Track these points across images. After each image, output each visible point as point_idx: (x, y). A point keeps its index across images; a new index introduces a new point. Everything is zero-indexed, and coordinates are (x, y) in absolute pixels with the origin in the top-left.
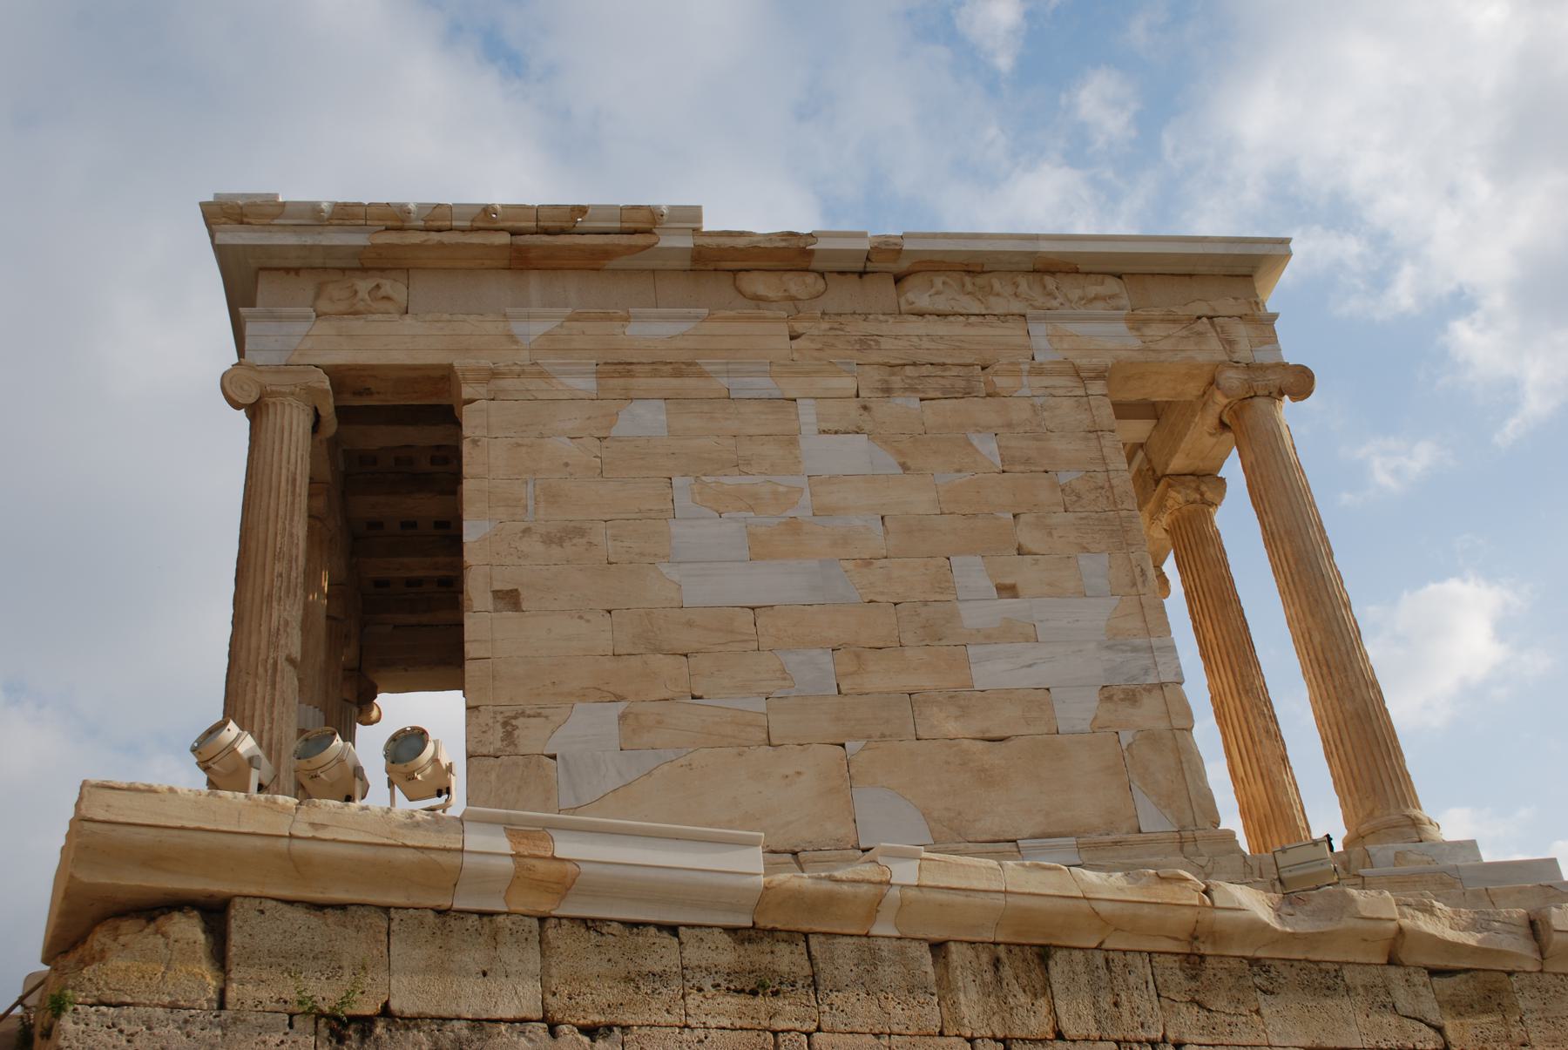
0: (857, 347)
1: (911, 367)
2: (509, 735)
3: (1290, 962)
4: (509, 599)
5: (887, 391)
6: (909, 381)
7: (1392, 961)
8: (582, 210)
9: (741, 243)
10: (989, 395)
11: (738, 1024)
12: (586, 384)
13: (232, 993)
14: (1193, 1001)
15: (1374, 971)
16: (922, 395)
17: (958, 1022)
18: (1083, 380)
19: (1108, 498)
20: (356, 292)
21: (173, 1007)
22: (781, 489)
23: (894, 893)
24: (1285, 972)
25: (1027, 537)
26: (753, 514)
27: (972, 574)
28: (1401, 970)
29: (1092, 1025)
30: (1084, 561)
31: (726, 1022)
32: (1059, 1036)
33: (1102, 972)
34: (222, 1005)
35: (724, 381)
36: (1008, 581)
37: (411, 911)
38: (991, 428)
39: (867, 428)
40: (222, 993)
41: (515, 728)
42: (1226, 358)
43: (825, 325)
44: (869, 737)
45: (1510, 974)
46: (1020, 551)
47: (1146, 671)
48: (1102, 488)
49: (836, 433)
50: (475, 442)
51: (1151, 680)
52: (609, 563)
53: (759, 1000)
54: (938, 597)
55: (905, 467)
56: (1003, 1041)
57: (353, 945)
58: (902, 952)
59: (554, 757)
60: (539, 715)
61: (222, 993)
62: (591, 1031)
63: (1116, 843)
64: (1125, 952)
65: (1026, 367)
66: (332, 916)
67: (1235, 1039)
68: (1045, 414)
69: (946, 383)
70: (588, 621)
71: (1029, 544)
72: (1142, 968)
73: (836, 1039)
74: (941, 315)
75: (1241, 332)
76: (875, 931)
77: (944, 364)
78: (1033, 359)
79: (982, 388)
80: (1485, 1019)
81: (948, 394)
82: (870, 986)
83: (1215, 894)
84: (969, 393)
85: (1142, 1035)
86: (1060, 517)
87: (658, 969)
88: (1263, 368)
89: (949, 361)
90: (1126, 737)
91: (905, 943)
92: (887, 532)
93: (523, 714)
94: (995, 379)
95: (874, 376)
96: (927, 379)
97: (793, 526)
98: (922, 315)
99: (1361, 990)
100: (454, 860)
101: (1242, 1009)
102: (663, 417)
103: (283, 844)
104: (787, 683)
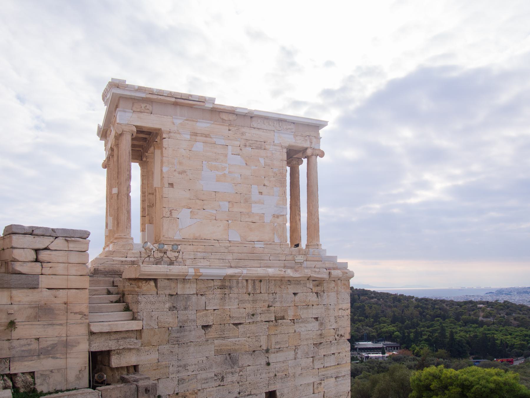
0: (241, 134)
1: (251, 141)
3: (294, 280)
5: (245, 146)
6: (250, 144)
7: (308, 279)
10: (264, 149)
11: (220, 293)
13: (158, 293)
14: (279, 287)
15: (305, 281)
16: (252, 148)
19: (282, 175)
22: (223, 166)
23: (243, 275)
24: (293, 282)
26: (217, 171)
28: (309, 281)
29: (265, 291)
31: (219, 293)
32: (261, 293)
33: (268, 283)
34: (157, 294)
37: (180, 279)
38: (264, 157)
39: (241, 154)
40: (157, 292)
42: (309, 146)
45: (324, 280)
47: (281, 212)
48: (281, 173)
49: (235, 155)
52: (190, 179)
53: (223, 290)
55: (246, 164)
56: (253, 294)
57: (173, 285)
58: (242, 282)
61: (157, 292)
62: (201, 295)
64: (272, 280)
65: (272, 144)
66: (170, 281)
67: (284, 292)
68: (274, 155)
70: (186, 191)
72: (273, 282)
73: (232, 295)
76: (239, 279)
77: (257, 141)
79: (263, 147)
80: (318, 287)
81: (257, 148)
83: (286, 272)
84: (261, 148)
85: (272, 292)
86: (272, 179)
87: (211, 286)
88: (316, 149)
89: (258, 140)
91: (243, 280)
92: (241, 179)
94: (266, 146)
96: (254, 144)
97: (224, 175)
99: (302, 284)
100: (187, 273)
101: (286, 288)
102: (202, 147)
103: (166, 273)
104: (219, 208)
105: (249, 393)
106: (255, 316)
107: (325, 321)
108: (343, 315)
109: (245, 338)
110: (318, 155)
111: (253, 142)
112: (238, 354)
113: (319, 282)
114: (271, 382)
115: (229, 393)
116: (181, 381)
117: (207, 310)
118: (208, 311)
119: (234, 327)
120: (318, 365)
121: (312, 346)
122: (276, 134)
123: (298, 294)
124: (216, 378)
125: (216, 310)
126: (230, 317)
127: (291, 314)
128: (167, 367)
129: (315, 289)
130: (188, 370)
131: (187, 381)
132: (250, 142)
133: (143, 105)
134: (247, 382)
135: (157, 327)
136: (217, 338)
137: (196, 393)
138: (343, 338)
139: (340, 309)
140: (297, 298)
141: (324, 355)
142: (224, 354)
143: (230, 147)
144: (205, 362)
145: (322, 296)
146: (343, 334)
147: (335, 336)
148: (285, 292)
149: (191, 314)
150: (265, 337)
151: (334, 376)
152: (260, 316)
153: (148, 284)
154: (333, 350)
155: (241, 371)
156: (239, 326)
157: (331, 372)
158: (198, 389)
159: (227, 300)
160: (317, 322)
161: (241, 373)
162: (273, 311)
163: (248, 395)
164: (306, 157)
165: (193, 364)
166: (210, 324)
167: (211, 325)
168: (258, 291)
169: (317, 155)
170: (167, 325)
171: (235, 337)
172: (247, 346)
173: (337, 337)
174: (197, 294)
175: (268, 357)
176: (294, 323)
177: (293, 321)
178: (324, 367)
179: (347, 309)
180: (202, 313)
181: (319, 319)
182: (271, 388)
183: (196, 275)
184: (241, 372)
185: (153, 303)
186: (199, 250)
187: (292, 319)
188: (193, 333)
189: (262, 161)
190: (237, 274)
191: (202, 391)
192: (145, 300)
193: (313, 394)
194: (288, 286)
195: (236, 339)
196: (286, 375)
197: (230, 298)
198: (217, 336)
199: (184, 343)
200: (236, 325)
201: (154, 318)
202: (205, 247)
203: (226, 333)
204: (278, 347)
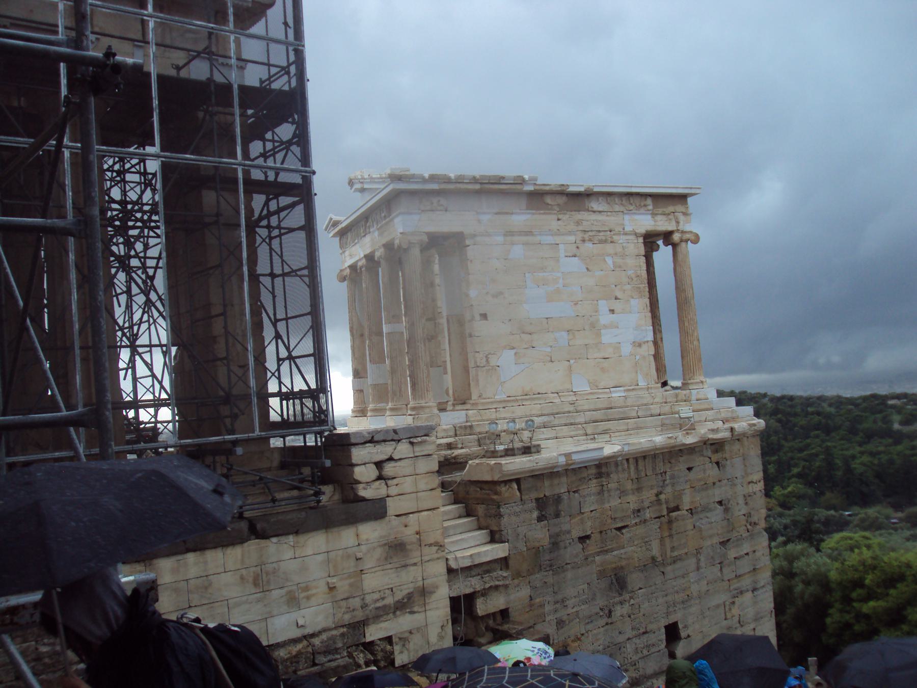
2: (487, 361)
4: (484, 316)
5: (584, 241)
7: (705, 444)
8: (503, 178)
9: (547, 188)
10: (611, 242)
12: (500, 239)
17: (630, 476)
18: (637, 237)
20: (432, 203)
21: (515, 502)
23: (624, 453)
25: (619, 295)
27: (603, 306)
30: (634, 302)
32: (646, 475)
34: (522, 500)
35: (539, 238)
36: (612, 309)
39: (578, 254)
41: (489, 358)
42: (675, 229)
43: (568, 216)
44: (576, 359)
46: (616, 298)
47: (644, 337)
50: (471, 261)
51: (645, 340)
53: (599, 480)
54: (594, 314)
55: (587, 269)
59: (498, 366)
60: (494, 354)
62: (574, 492)
63: (633, 389)
69: (600, 238)
71: (619, 297)
74: (600, 212)
75: (682, 218)
78: (624, 229)
79: (610, 239)
81: (601, 242)
82: (617, 472)
86: (629, 287)
88: (686, 232)
90: (638, 357)
93: (490, 354)
94: (614, 237)
95: (580, 235)
98: (594, 212)
105: (644, 630)
106: (642, 513)
107: (732, 505)
108: (754, 490)
109: (632, 548)
110: (689, 240)
111: (593, 233)
112: (626, 573)
113: (717, 446)
114: (671, 609)
115: (620, 633)
116: (560, 623)
117: (583, 513)
118: (585, 515)
119: (618, 533)
120: (728, 573)
121: (718, 546)
122: (627, 217)
123: (693, 469)
124: (601, 614)
125: (593, 512)
126: (612, 518)
127: (686, 502)
128: (542, 606)
129: (715, 458)
130: (567, 606)
131: (567, 622)
132: (590, 233)
133: (435, 200)
134: (641, 614)
135: (525, 549)
136: (599, 553)
137: (579, 639)
138: (758, 527)
139: (749, 483)
140: (692, 475)
141: (735, 558)
142: (608, 575)
143: (561, 246)
144: (586, 591)
145: (724, 466)
146: (757, 522)
147: (746, 526)
148: (677, 468)
149: (565, 523)
150: (658, 541)
151: (750, 588)
152: (648, 511)
153: (510, 487)
154: (746, 548)
155: (631, 598)
156: (624, 531)
157: (746, 582)
158: (582, 633)
159: (606, 494)
160: (722, 507)
161: (632, 602)
162: (663, 501)
163: (644, 633)
164: (669, 245)
165: (572, 596)
166: (589, 533)
167: (589, 535)
168: (643, 474)
169: (686, 241)
170: (537, 544)
171: (619, 548)
172: (636, 559)
173: (749, 527)
174: (569, 492)
175: (663, 573)
176: (692, 514)
177: (690, 511)
178: (736, 576)
179: (760, 481)
180: (577, 519)
181: (723, 502)
182: (672, 619)
183: (567, 465)
184: (632, 600)
185: (516, 514)
186: (534, 412)
187: (688, 508)
188: (569, 550)
189: (609, 261)
190: (617, 454)
191: (586, 634)
192: (508, 511)
193: (726, 619)
194: (680, 458)
195: (622, 551)
196: (688, 595)
197: (609, 491)
198: (599, 550)
199: (559, 568)
200: (619, 529)
201: (521, 537)
202: (542, 405)
203: (608, 544)
204: (676, 554)
